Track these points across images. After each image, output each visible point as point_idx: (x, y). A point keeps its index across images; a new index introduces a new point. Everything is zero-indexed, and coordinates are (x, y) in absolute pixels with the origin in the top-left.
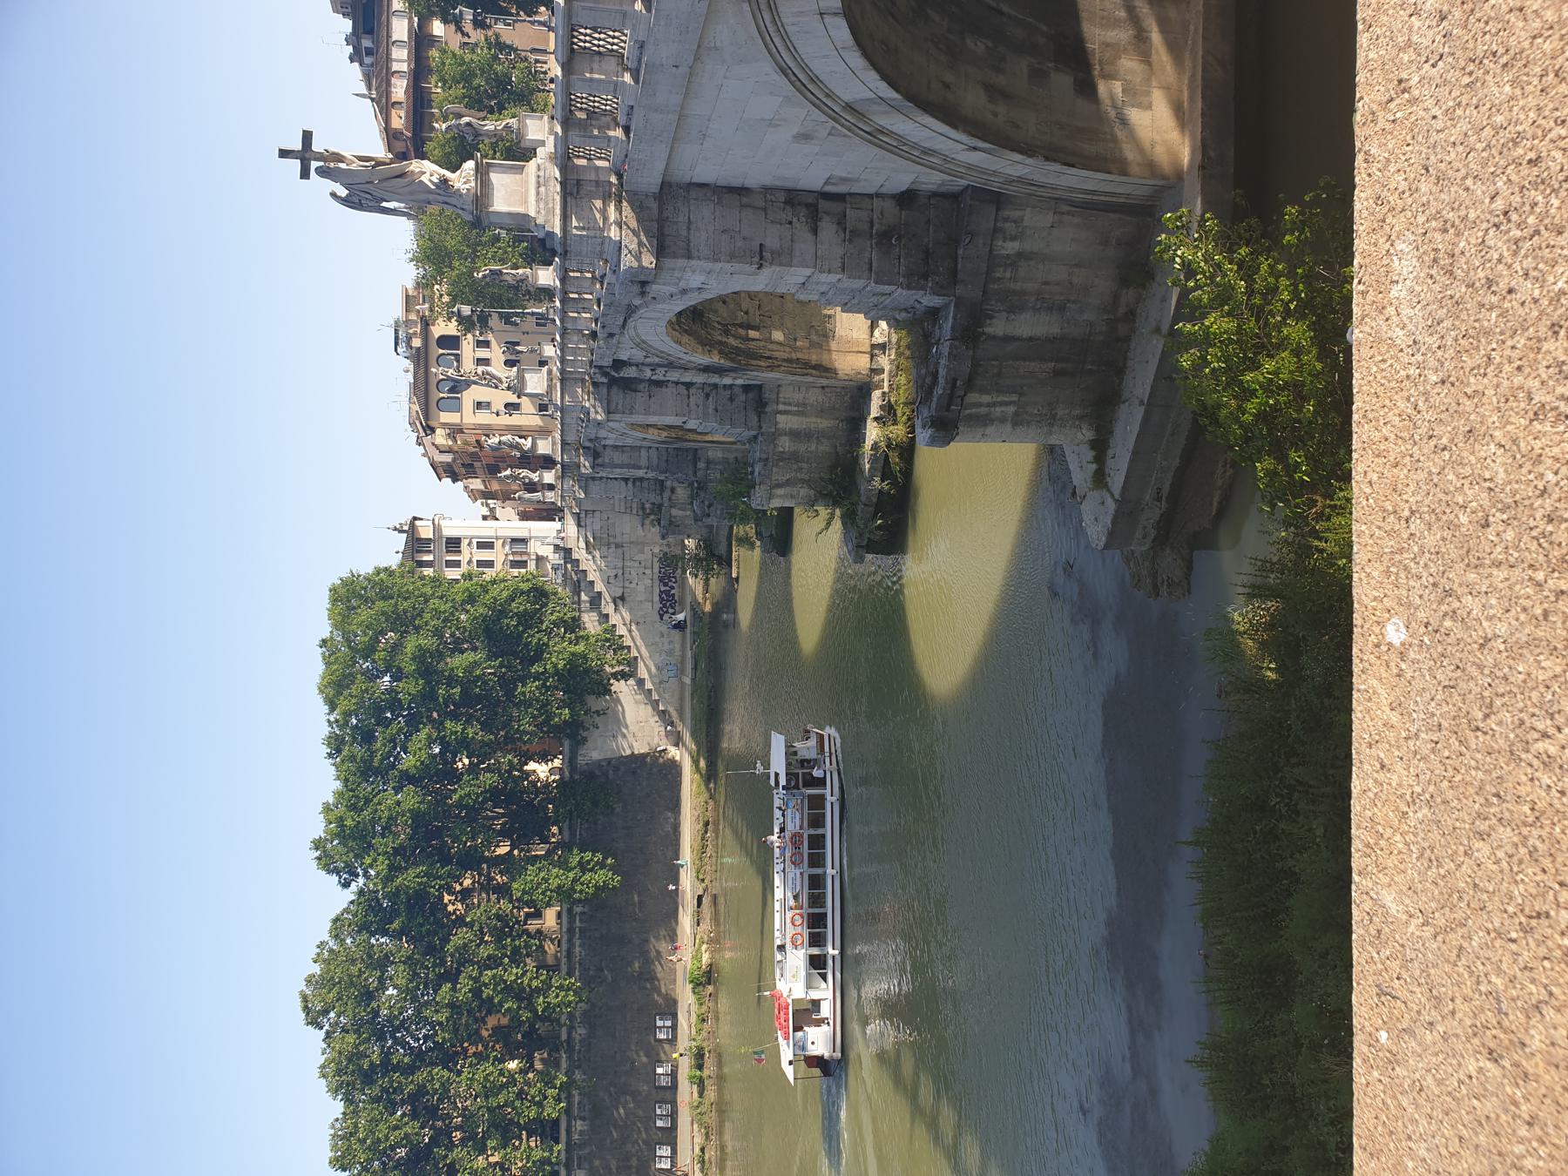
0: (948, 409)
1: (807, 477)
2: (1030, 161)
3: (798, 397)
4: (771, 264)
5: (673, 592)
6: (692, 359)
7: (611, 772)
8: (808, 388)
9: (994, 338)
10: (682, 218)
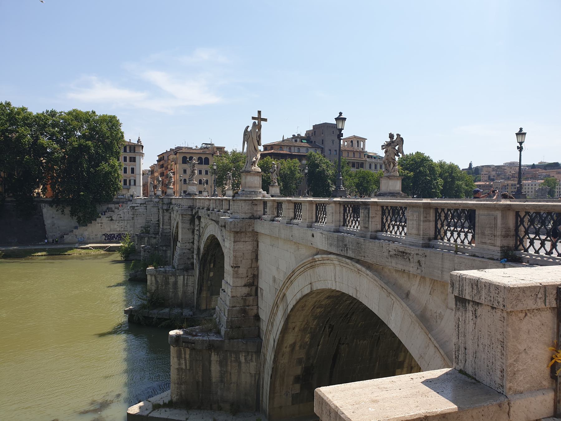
0: (183, 342)
1: (159, 289)
2: (272, 362)
3: (190, 283)
4: (233, 271)
5: (114, 239)
6: (202, 244)
8: (193, 287)
9: (210, 356)
10: (247, 239)
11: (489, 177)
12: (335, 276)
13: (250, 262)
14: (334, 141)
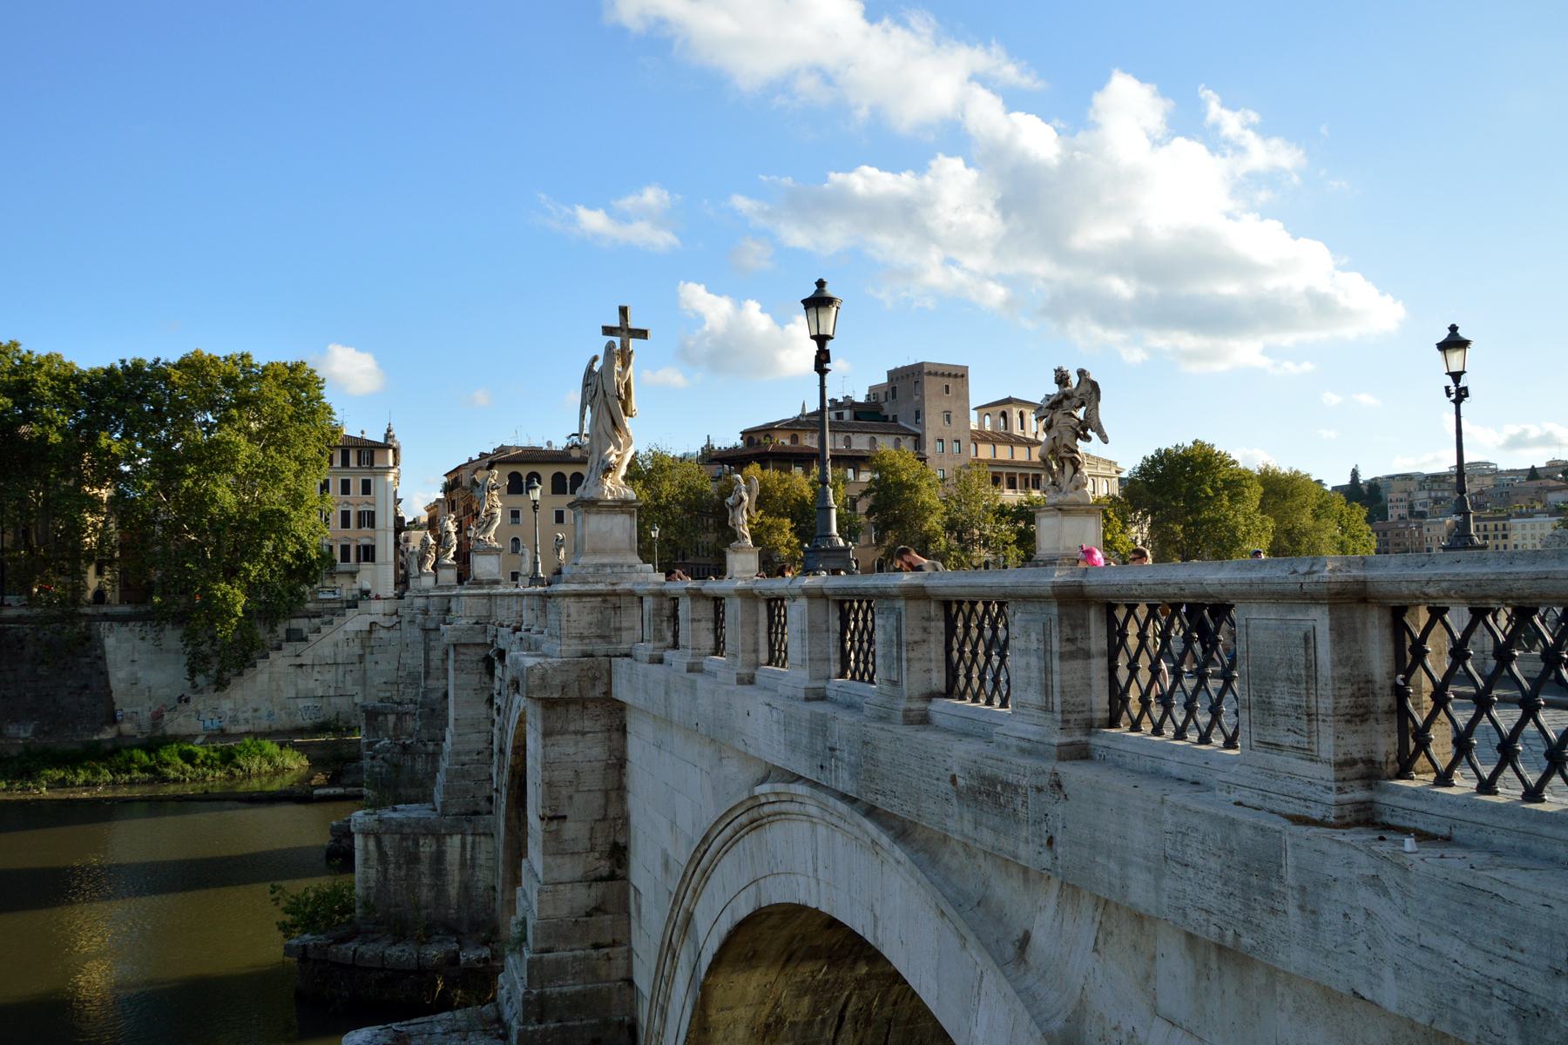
1: (390, 876)
3: (482, 858)
4: (545, 831)
7: (88, 660)
8: (490, 869)
10: (588, 724)
11: (1411, 506)
12: (815, 858)
13: (601, 802)
14: (952, 415)
